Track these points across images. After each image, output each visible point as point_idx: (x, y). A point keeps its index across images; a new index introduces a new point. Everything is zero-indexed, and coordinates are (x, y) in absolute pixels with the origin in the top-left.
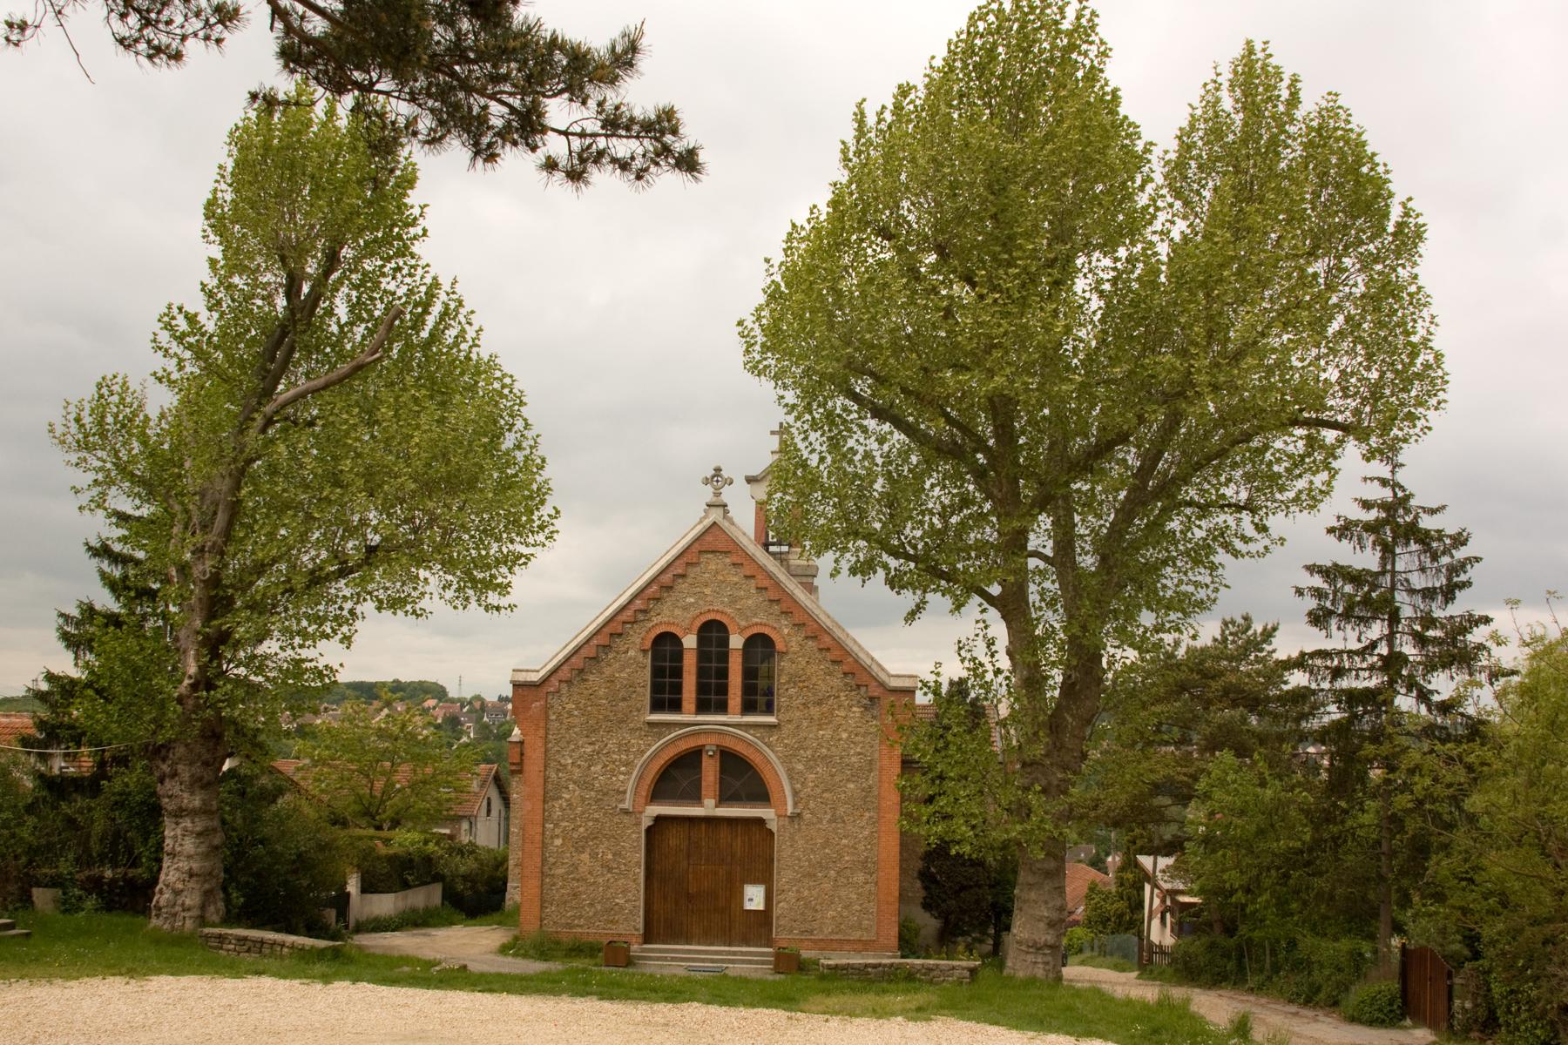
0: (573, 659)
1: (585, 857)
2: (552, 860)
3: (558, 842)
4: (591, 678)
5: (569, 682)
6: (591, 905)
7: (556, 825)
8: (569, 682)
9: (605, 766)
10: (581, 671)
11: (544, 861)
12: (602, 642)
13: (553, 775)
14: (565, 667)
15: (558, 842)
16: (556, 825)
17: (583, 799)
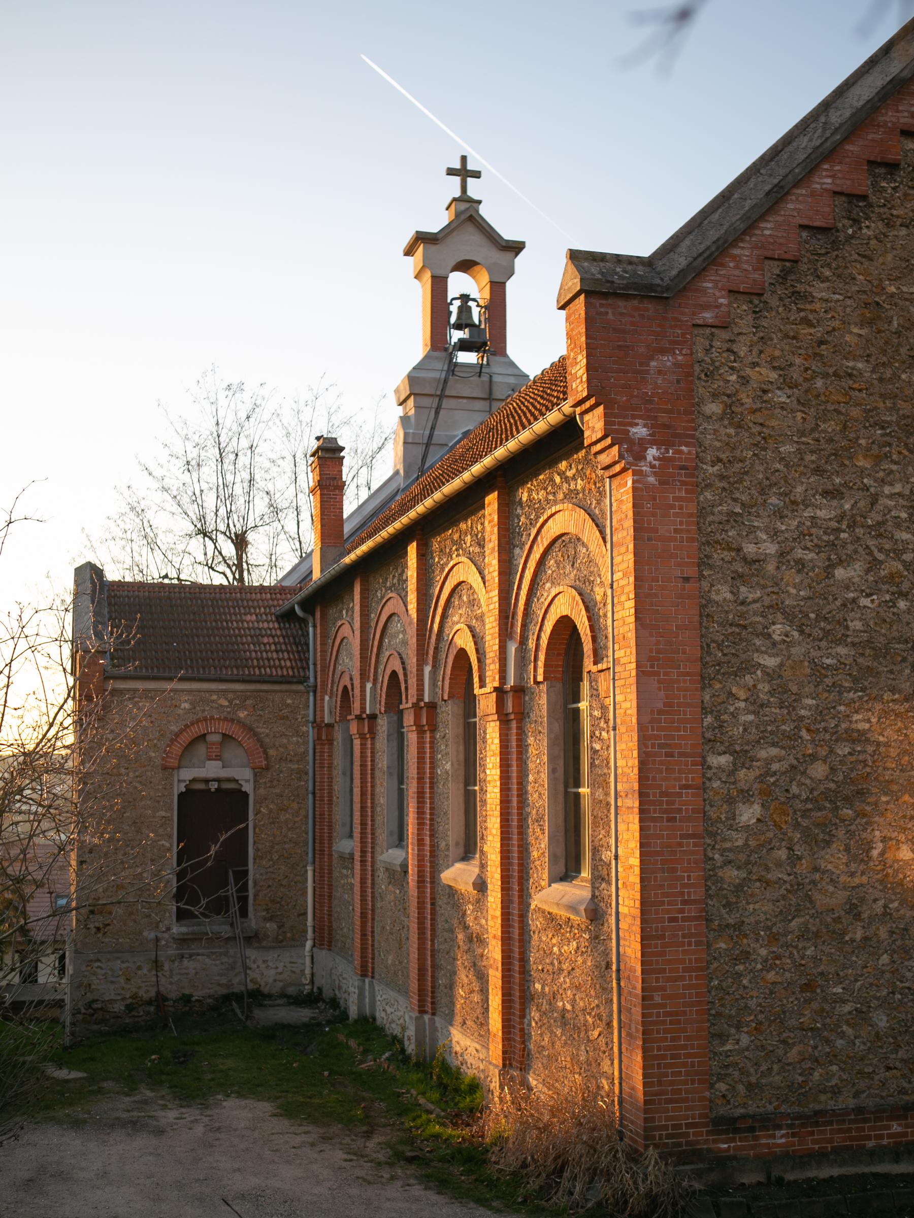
0: (767, 228)
1: (834, 859)
2: (732, 874)
3: (749, 814)
4: (819, 291)
5: (754, 295)
6: (861, 1016)
7: (743, 758)
8: (754, 295)
9: (874, 565)
10: (789, 268)
11: (711, 877)
12: (846, 185)
13: (723, 593)
14: (743, 251)
15: (749, 814)
16: (743, 758)
17: (818, 671)
